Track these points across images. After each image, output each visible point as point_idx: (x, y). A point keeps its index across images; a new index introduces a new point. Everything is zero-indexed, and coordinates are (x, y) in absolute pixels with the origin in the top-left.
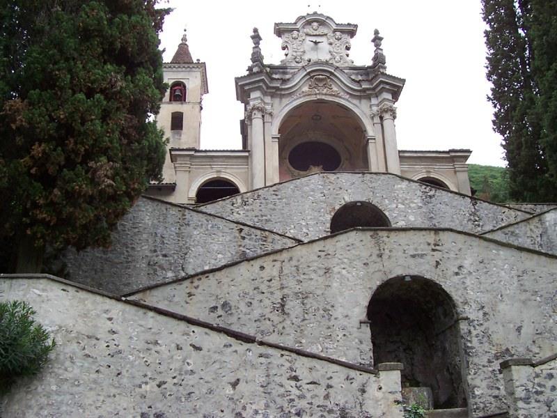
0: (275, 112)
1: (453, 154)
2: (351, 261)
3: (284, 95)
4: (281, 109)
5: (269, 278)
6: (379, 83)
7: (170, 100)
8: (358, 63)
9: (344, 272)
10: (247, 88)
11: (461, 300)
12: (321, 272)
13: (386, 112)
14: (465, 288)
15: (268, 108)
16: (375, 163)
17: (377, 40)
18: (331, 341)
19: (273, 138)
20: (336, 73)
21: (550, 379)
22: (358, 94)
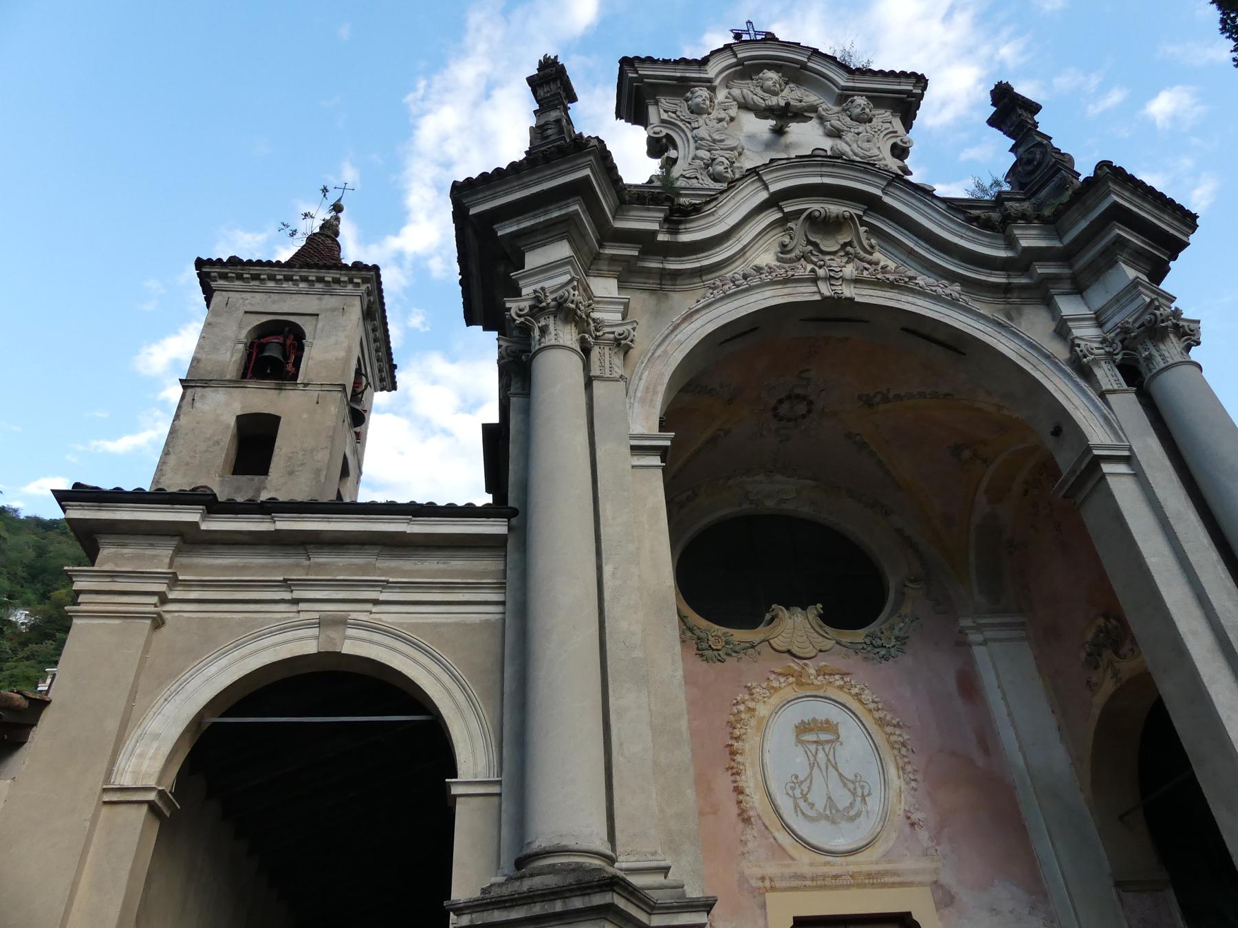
3: (676, 275)
4: (672, 333)
7: (244, 376)
10: (505, 230)
15: (610, 316)
19: (634, 449)
20: (887, 199)
22: (998, 278)
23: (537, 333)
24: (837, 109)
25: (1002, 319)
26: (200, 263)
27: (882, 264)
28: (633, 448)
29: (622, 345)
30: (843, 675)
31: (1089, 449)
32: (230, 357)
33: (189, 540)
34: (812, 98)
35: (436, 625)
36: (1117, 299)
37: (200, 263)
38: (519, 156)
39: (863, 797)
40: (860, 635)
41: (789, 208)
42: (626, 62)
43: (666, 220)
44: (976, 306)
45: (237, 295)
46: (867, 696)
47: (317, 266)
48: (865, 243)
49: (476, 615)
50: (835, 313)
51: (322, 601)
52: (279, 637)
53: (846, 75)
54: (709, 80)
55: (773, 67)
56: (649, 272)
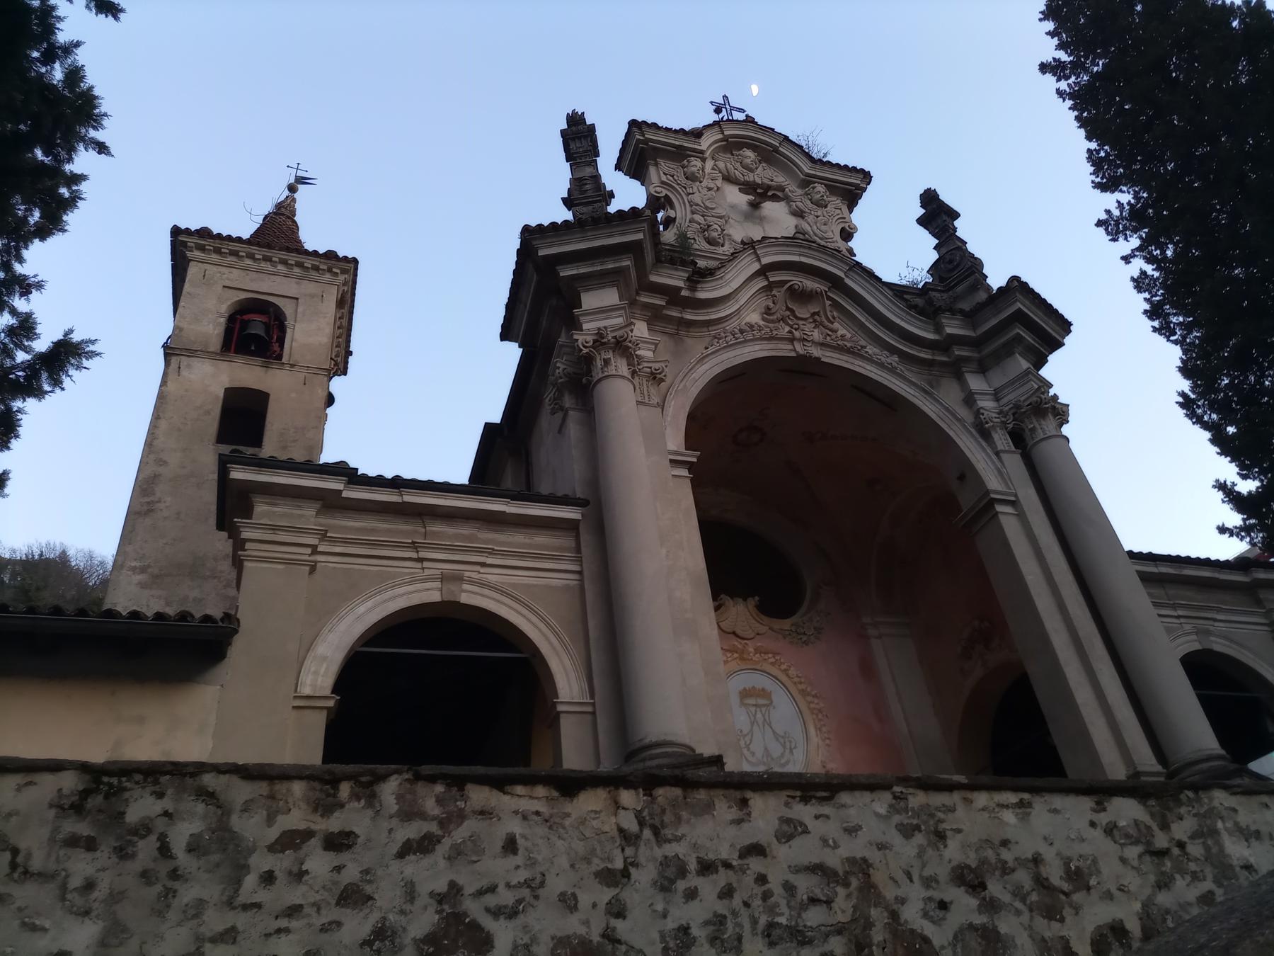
10: (566, 272)
20: (847, 281)
22: (925, 355)
23: (599, 363)
24: (800, 192)
25: (928, 388)
26: (176, 231)
27: (840, 333)
28: (671, 461)
30: (775, 654)
31: (988, 492)
32: (212, 329)
34: (780, 179)
35: (528, 586)
36: (1012, 382)
37: (176, 231)
39: (791, 750)
40: (786, 624)
41: (774, 277)
42: (633, 124)
43: (688, 279)
44: (907, 374)
45: (215, 268)
46: (792, 672)
48: (829, 314)
49: (557, 581)
50: (804, 368)
52: (411, 590)
53: (810, 164)
54: (702, 152)
55: (753, 149)
56: (670, 319)
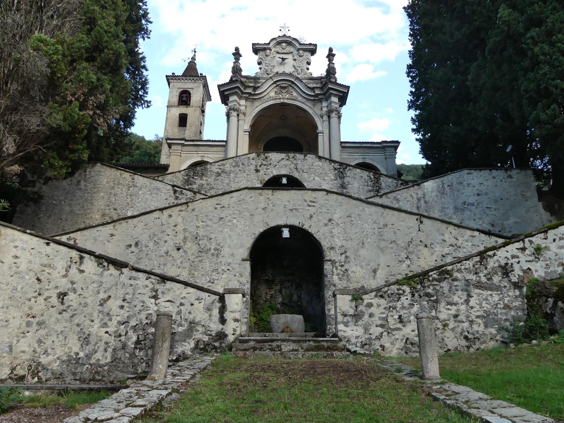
0: (248, 112)
1: (385, 145)
2: (240, 213)
3: (255, 99)
5: (175, 224)
6: (331, 91)
7: (179, 104)
8: (315, 75)
9: (235, 221)
10: (226, 93)
11: (327, 246)
12: (215, 220)
13: (332, 112)
14: (332, 237)
15: (242, 108)
16: (323, 150)
17: (331, 56)
18: (218, 273)
20: (295, 82)
21: (370, 308)
22: (312, 98)
25: (311, 106)
26: (167, 76)
29: (244, 114)
32: (176, 100)
33: (183, 145)
37: (167, 76)
38: (228, 81)
47: (193, 76)
50: (283, 105)
51: (201, 153)
